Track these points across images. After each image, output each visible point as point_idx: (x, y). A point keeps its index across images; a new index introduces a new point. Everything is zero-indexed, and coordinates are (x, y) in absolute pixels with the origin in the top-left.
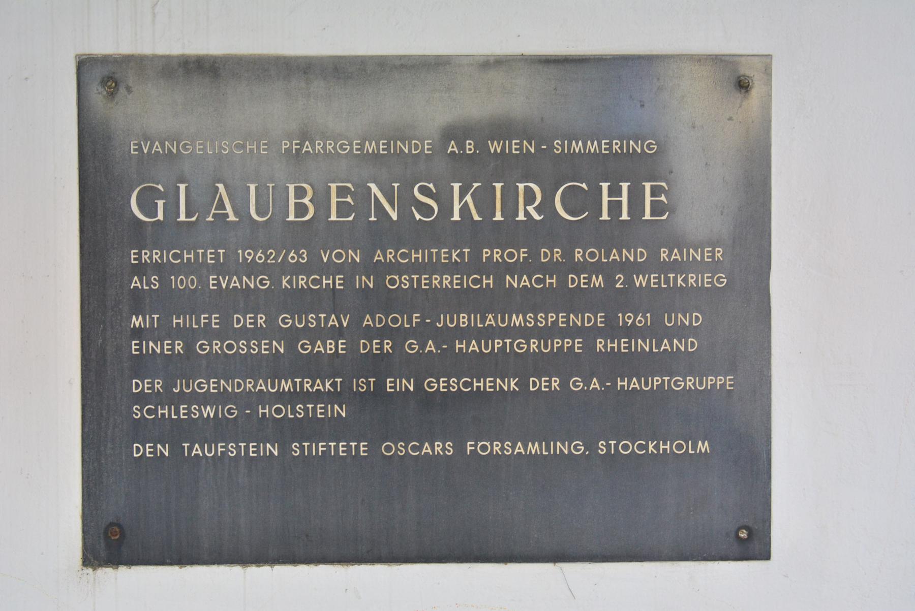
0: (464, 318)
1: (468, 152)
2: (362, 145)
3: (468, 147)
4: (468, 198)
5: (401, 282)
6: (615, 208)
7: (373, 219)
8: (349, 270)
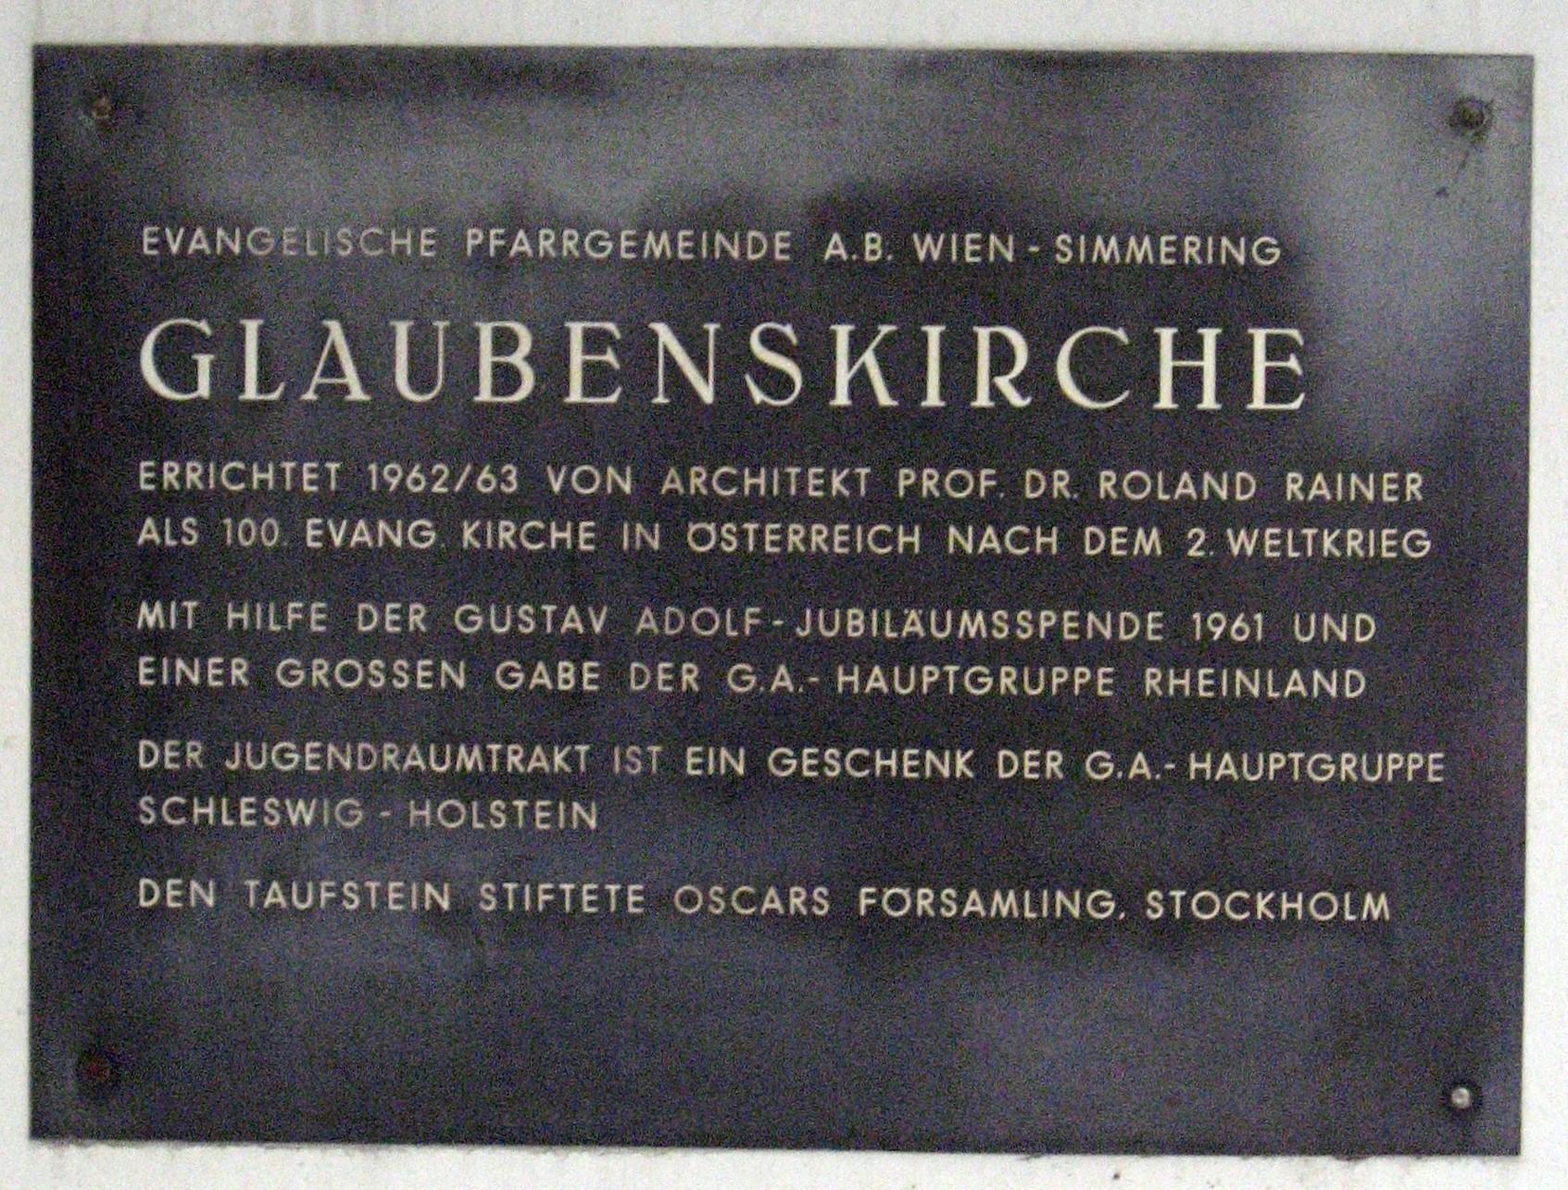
0: (855, 617)
1: (868, 258)
2: (640, 239)
3: (868, 247)
4: (869, 358)
5: (720, 539)
6: (1188, 383)
7: (661, 399)
8: (609, 510)
